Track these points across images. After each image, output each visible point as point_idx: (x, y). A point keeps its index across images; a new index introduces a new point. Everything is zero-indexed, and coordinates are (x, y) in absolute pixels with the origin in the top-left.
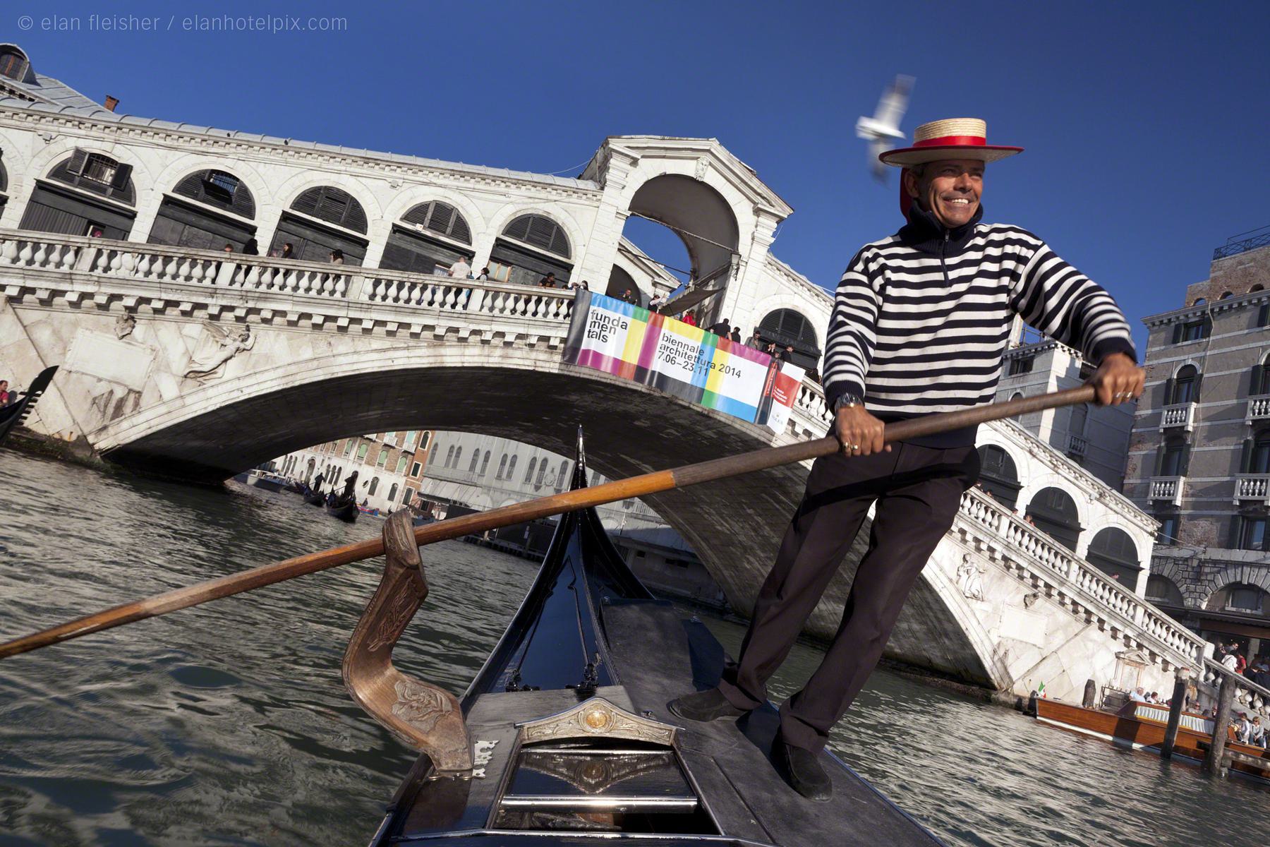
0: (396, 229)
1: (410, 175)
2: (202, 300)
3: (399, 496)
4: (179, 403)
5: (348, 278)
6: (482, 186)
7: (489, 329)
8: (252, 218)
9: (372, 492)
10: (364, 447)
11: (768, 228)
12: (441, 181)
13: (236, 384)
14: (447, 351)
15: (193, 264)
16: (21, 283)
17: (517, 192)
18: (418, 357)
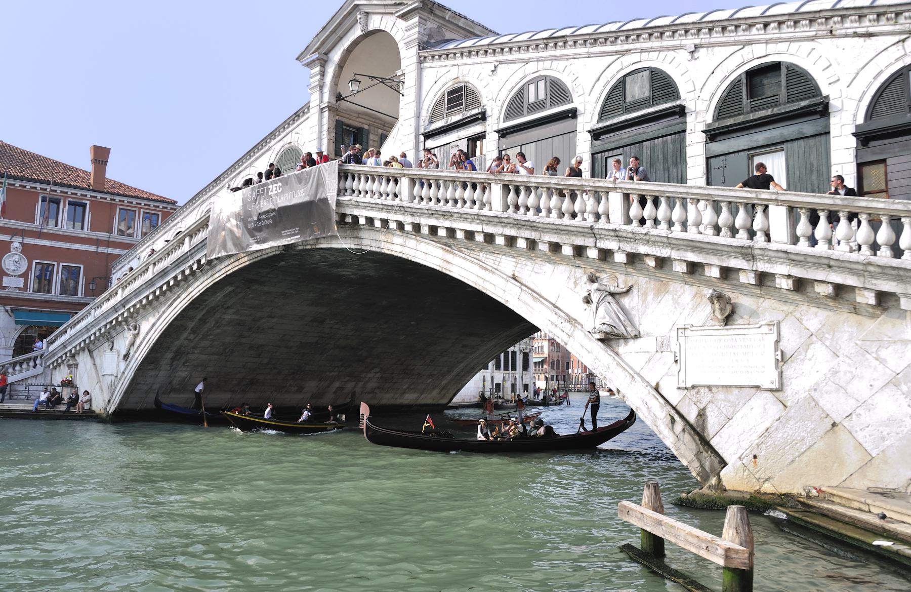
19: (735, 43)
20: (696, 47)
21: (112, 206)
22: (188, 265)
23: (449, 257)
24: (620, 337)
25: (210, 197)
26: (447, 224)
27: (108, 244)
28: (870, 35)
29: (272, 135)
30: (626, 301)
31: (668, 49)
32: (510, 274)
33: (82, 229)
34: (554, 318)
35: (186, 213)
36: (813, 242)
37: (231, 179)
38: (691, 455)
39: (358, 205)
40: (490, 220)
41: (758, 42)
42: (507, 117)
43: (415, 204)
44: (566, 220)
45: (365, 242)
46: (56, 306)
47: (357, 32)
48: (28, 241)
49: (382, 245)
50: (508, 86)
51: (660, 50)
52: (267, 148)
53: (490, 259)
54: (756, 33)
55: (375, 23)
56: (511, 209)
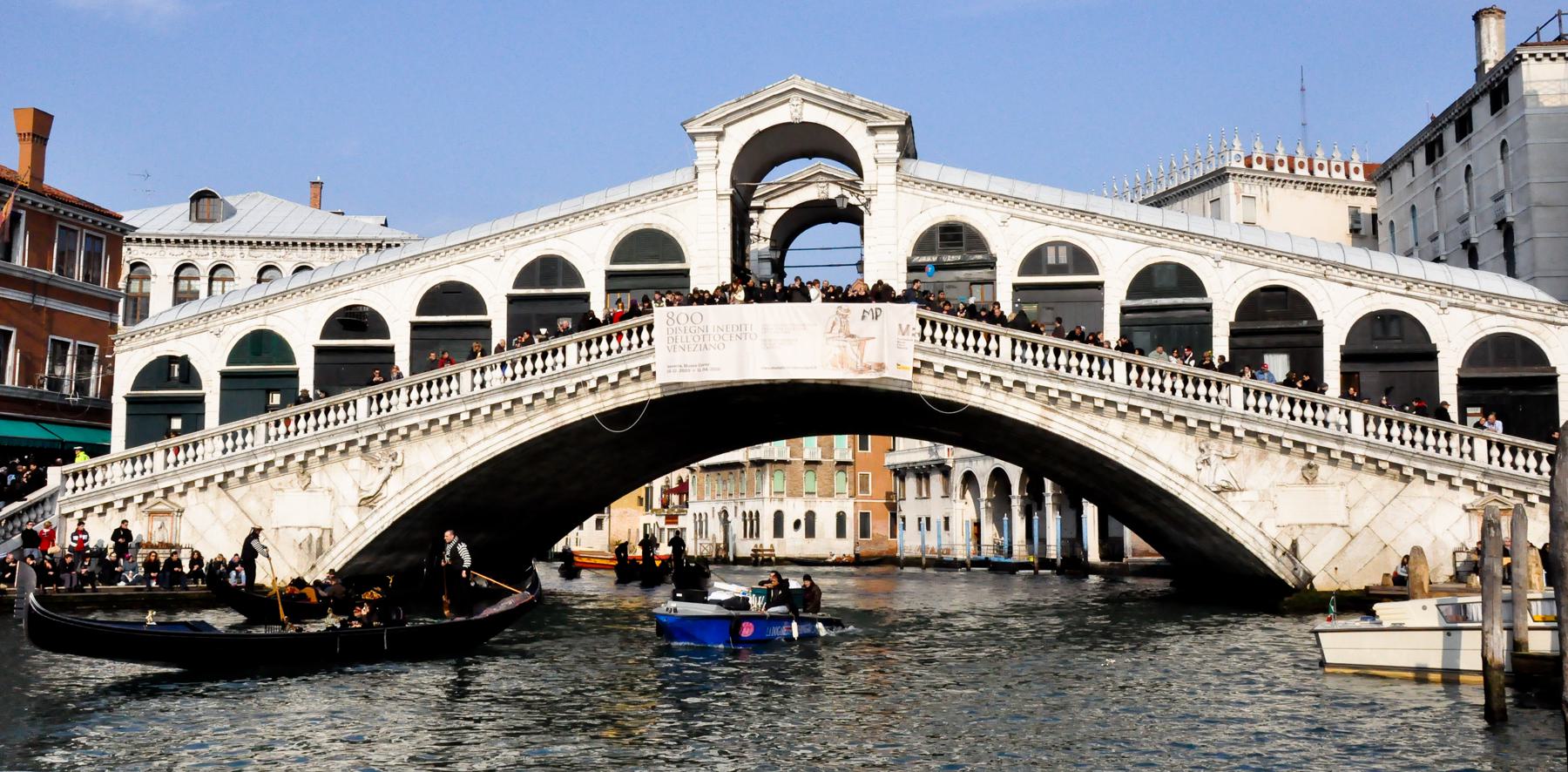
1: (509, 242)
2: (351, 437)
3: (851, 527)
4: (361, 528)
5: (458, 375)
6: (577, 224)
7: (591, 378)
8: (386, 335)
9: (810, 533)
10: (778, 475)
11: (890, 141)
12: (539, 234)
13: (399, 499)
15: (337, 410)
16: (223, 470)
17: (613, 216)
18: (541, 424)
20: (1224, 258)
24: (1230, 489)
26: (1063, 387)
27: (46, 289)
28: (1350, 284)
30: (1232, 464)
32: (1119, 435)
33: (8, 257)
34: (1170, 474)
36: (1378, 437)
38: (1288, 573)
40: (1119, 391)
42: (1022, 273)
45: (925, 388)
49: (953, 393)
52: (597, 218)
53: (1097, 420)
56: (1134, 384)
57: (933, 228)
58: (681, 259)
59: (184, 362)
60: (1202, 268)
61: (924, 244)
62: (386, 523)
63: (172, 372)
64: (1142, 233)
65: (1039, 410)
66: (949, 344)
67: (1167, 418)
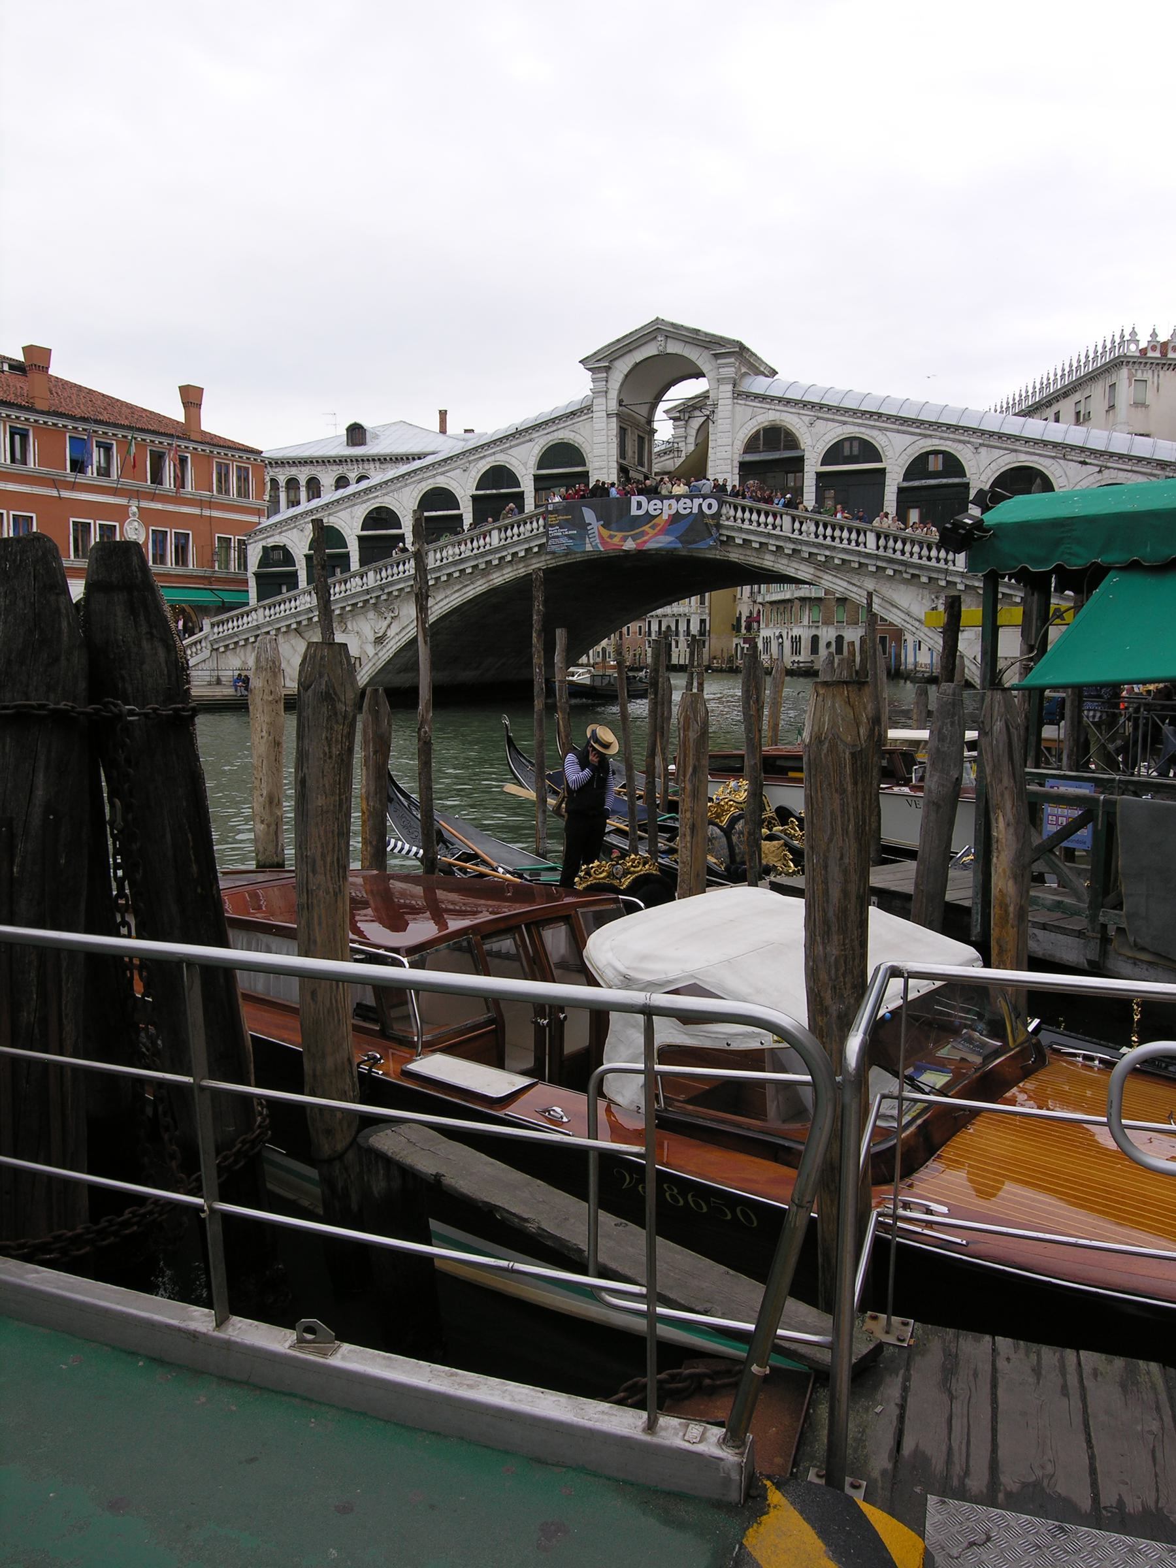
0: (475, 498)
10: (816, 609)
13: (397, 638)
14: (495, 576)
16: (294, 620)
19: (1006, 449)
21: (209, 457)
22: (498, 556)
23: (819, 574)
25: (434, 476)
26: (827, 553)
28: (1084, 463)
29: (536, 427)
31: (960, 441)
34: (907, 618)
35: (389, 489)
37: (470, 462)
39: (741, 530)
41: (1020, 451)
43: (796, 535)
44: (924, 562)
45: (731, 555)
46: (173, 579)
47: (650, 350)
48: (144, 504)
49: (752, 559)
50: (828, 438)
51: (954, 440)
54: (1018, 446)
55: (674, 348)
57: (758, 432)
58: (583, 463)
59: (284, 549)
60: (964, 454)
61: (751, 445)
62: (391, 654)
63: (278, 556)
64: (918, 427)
65: (812, 571)
66: (747, 522)
67: (905, 575)
